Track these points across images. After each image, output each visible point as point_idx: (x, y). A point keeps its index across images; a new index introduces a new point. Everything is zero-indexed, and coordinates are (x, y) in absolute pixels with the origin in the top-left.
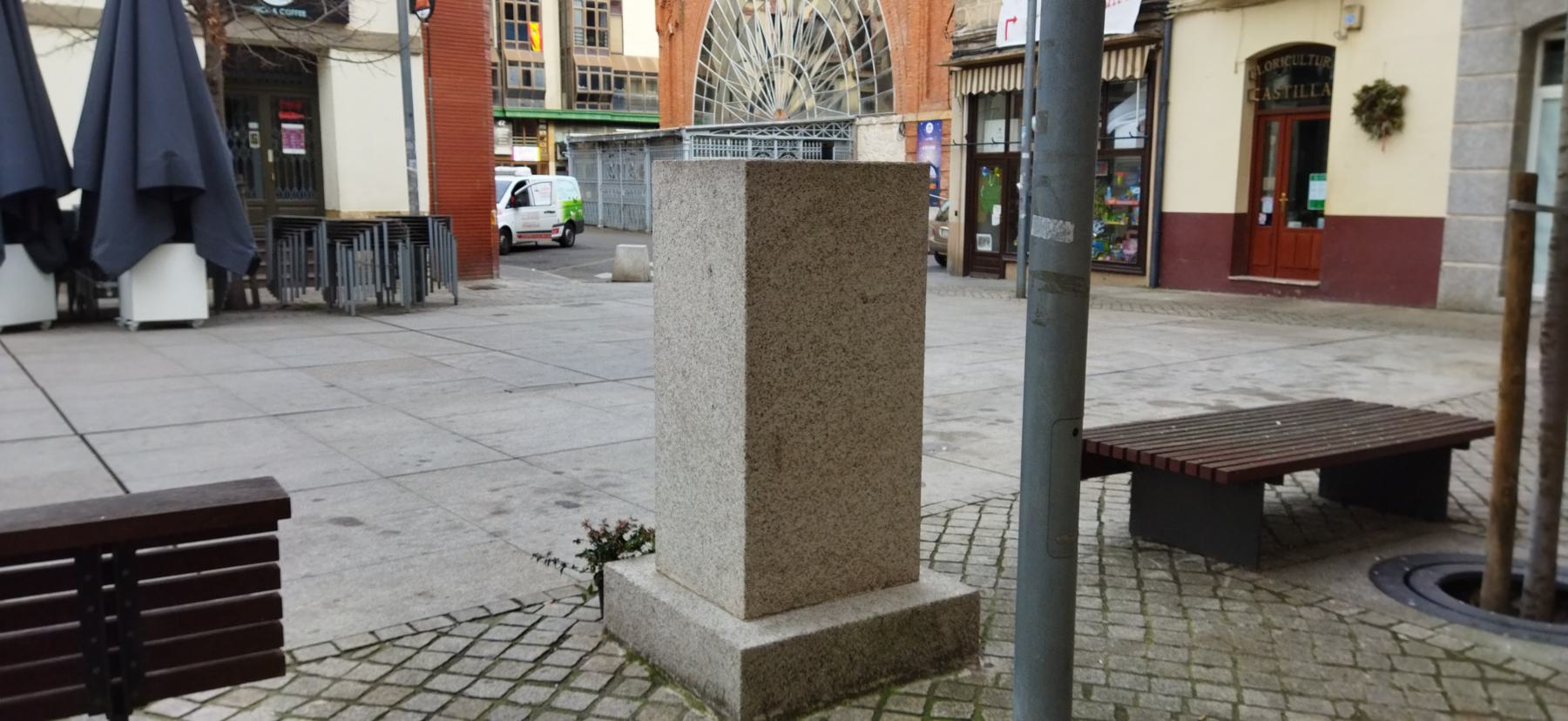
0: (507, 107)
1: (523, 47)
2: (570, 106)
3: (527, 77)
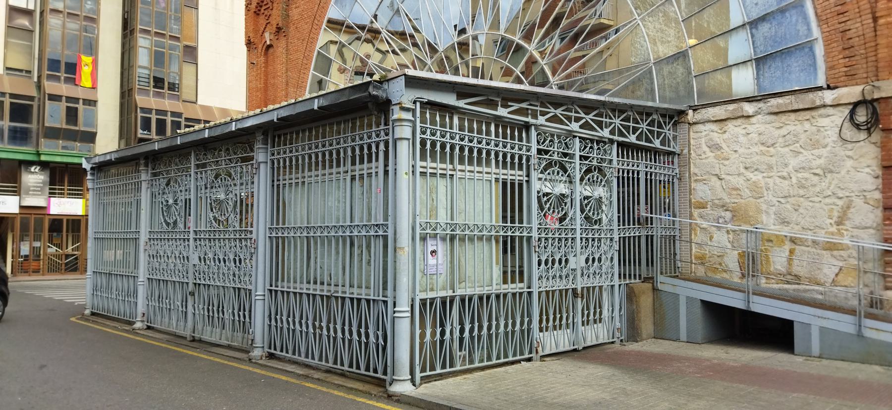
0: (43, 149)
1: (68, 80)
3: (72, 115)
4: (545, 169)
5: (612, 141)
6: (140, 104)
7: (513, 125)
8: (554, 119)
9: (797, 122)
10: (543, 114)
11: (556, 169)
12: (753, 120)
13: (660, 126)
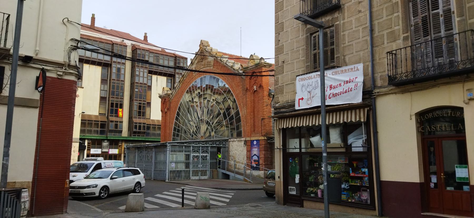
0: (108, 136)
1: (115, 116)
2: (130, 136)
3: (116, 126)
6: (134, 121)
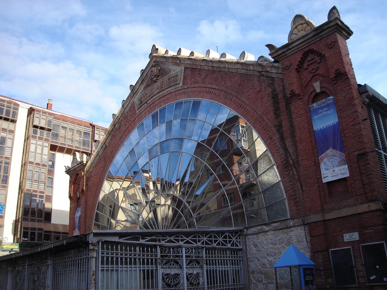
4: (166, 264)
5: (202, 248)
7: (148, 246)
8: (170, 241)
9: (282, 234)
10: (163, 240)
11: (172, 263)
12: (268, 233)
13: (230, 238)
